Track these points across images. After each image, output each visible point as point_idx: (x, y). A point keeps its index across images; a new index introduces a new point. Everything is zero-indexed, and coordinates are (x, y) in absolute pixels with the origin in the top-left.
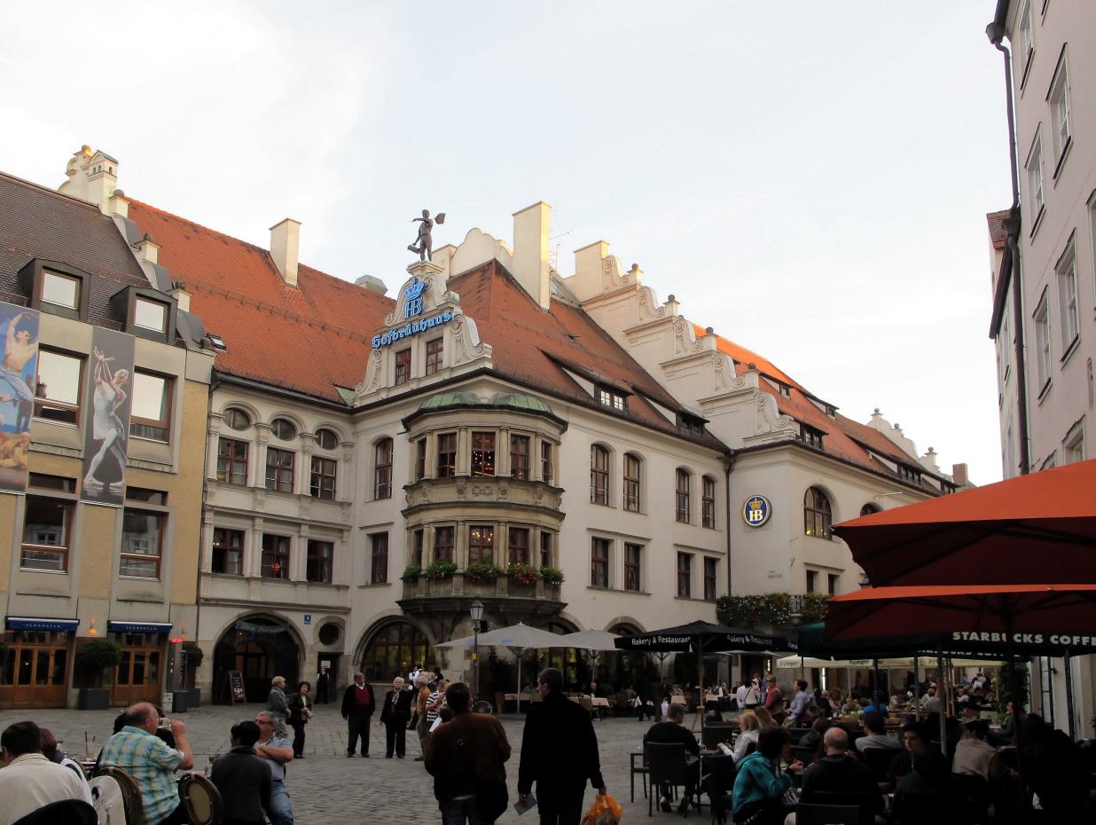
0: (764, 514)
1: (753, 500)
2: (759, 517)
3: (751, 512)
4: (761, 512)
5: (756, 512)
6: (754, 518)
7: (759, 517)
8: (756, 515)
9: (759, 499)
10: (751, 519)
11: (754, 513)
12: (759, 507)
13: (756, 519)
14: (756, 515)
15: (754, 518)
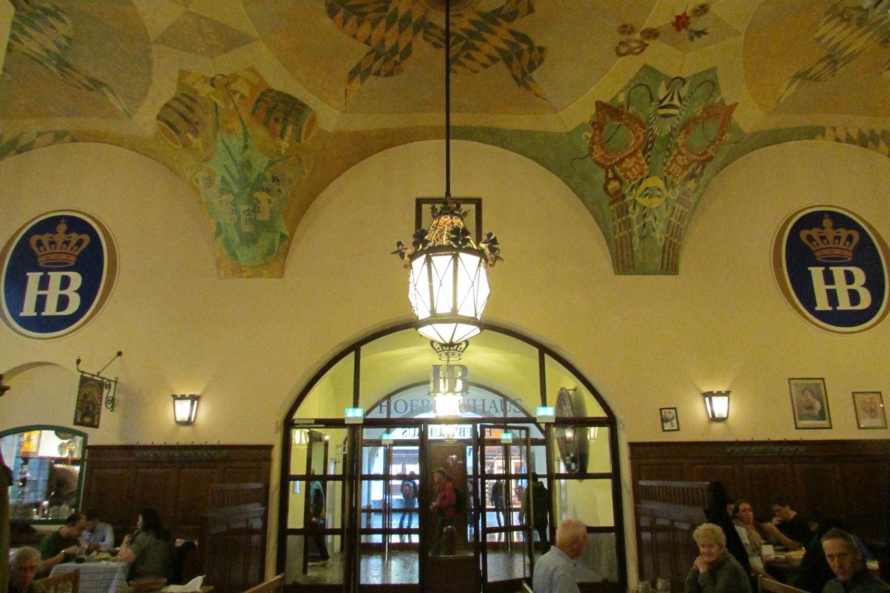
0: (88, 293)
1: (48, 225)
2: (63, 302)
3: (34, 278)
4: (76, 280)
5: (55, 277)
6: (41, 302)
7: (63, 302)
8: (53, 293)
9: (76, 225)
10: (29, 310)
11: (44, 284)
12: (72, 260)
13: (51, 310)
14: (53, 293)
15: (41, 302)
